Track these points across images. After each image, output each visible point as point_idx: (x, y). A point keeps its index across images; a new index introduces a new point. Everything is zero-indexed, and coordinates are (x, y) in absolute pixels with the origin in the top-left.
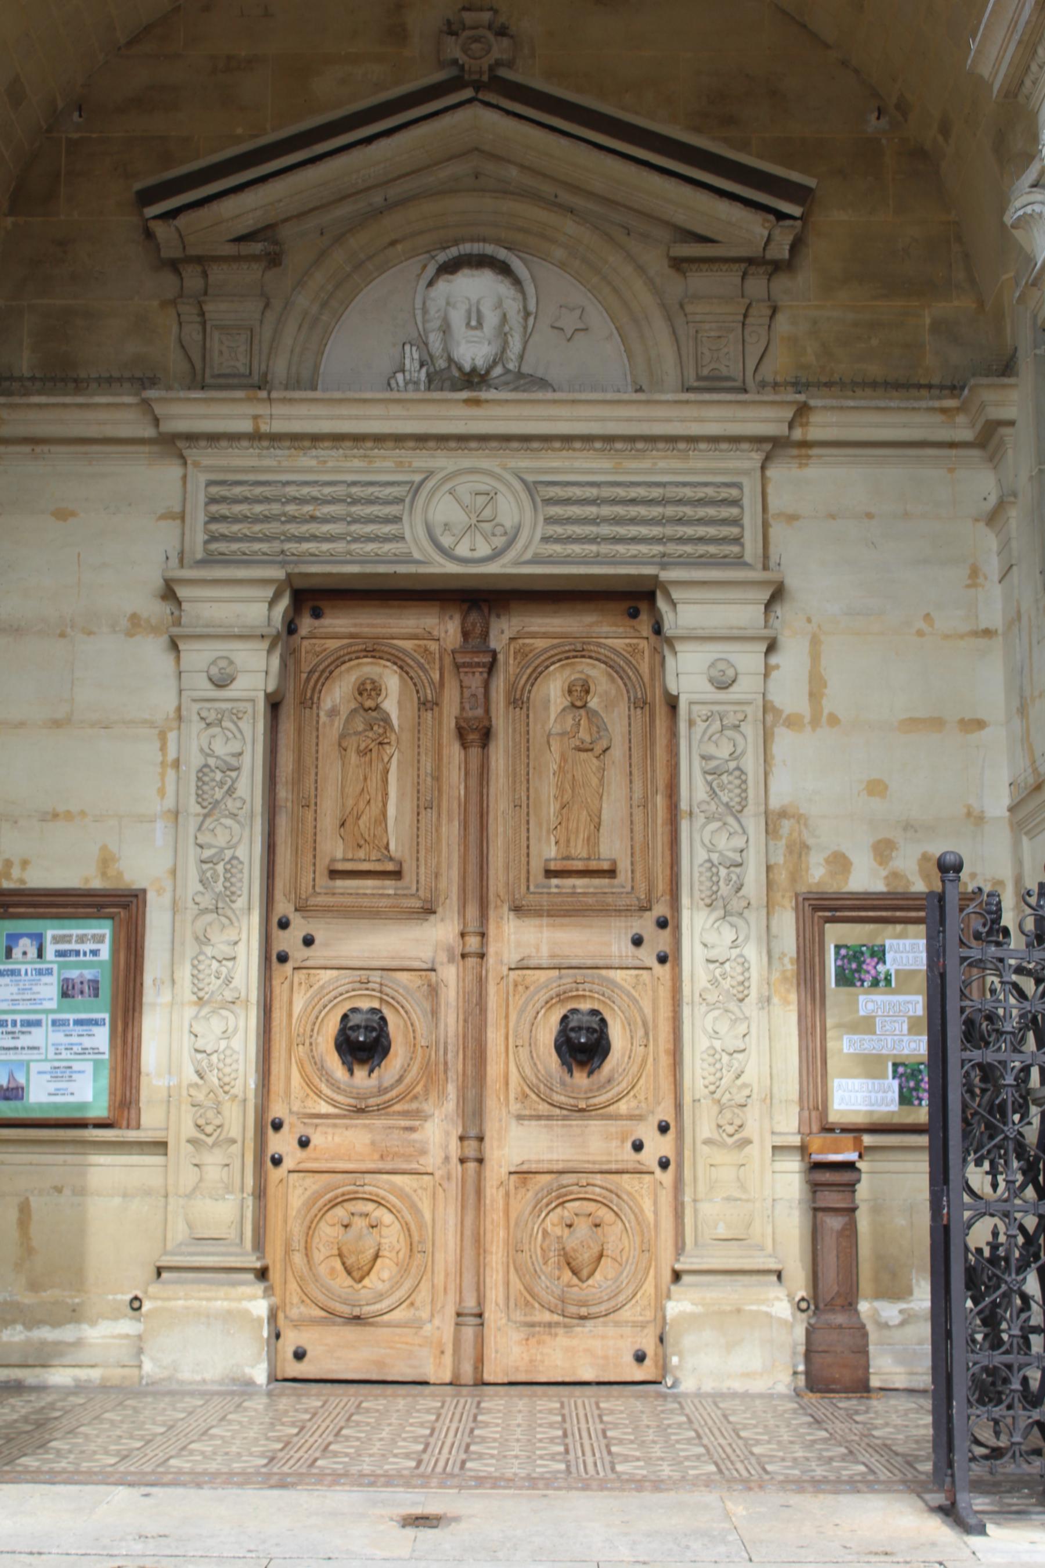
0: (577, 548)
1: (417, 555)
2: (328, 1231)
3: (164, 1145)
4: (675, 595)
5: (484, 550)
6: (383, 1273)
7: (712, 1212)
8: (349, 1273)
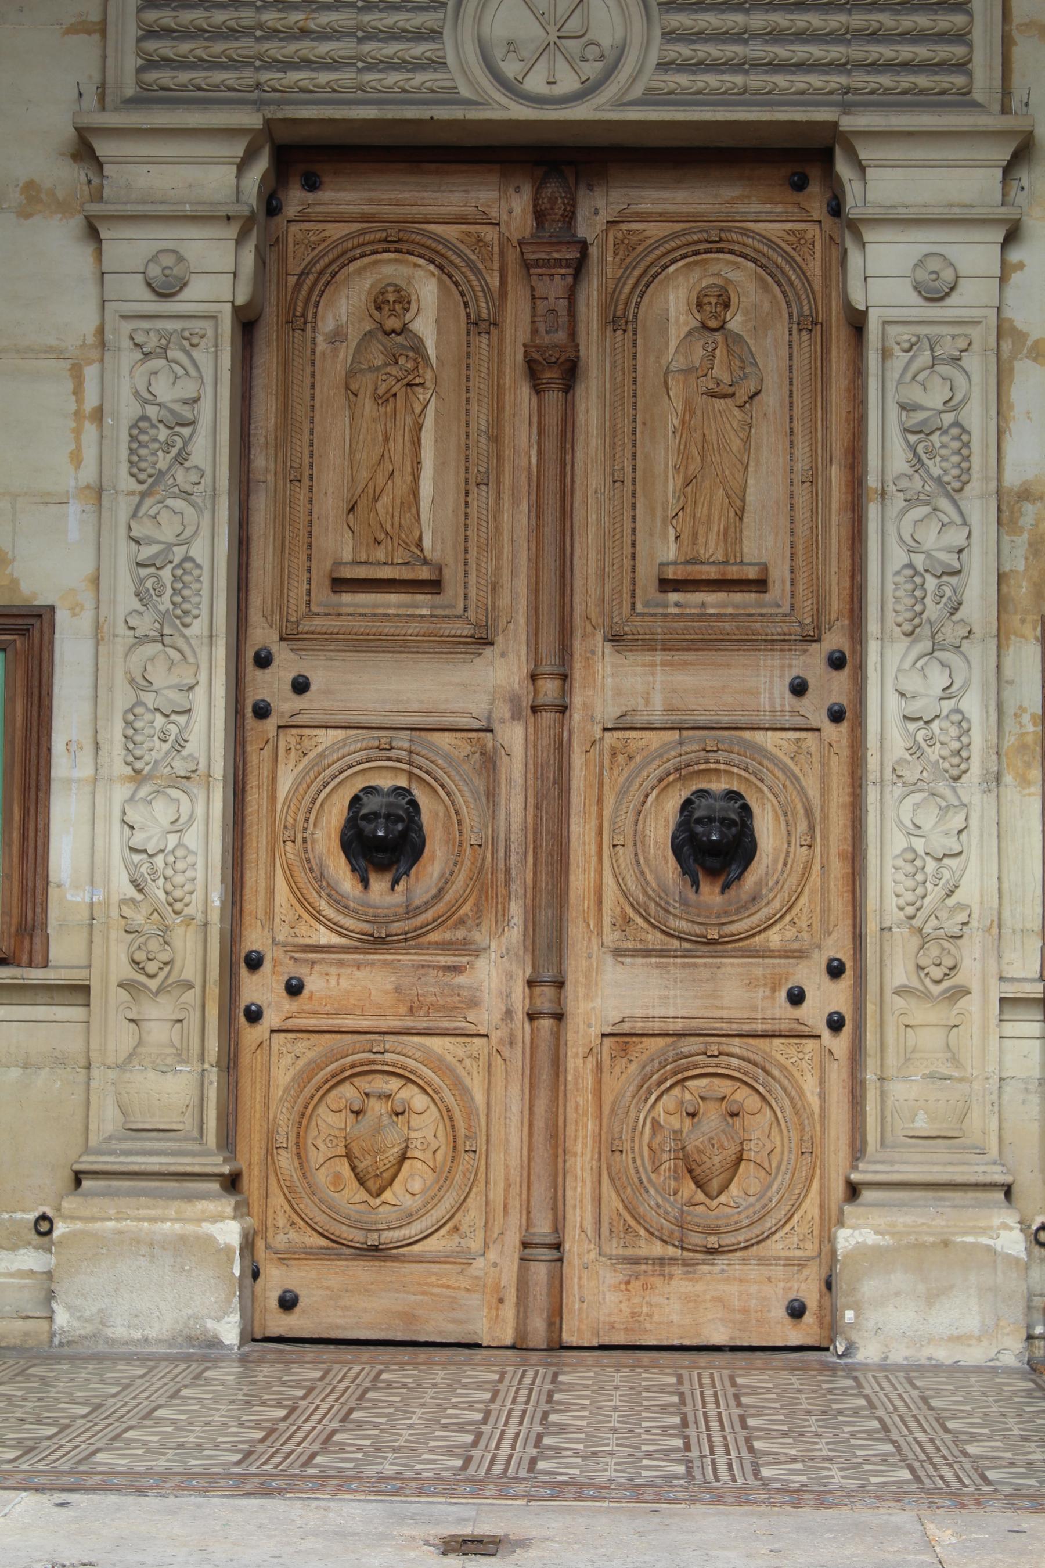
0: (712, 80)
1: (465, 92)
2: (330, 1120)
3: (85, 989)
4: (864, 154)
5: (568, 83)
6: (415, 1179)
7: (907, 1099)
8: (362, 1182)
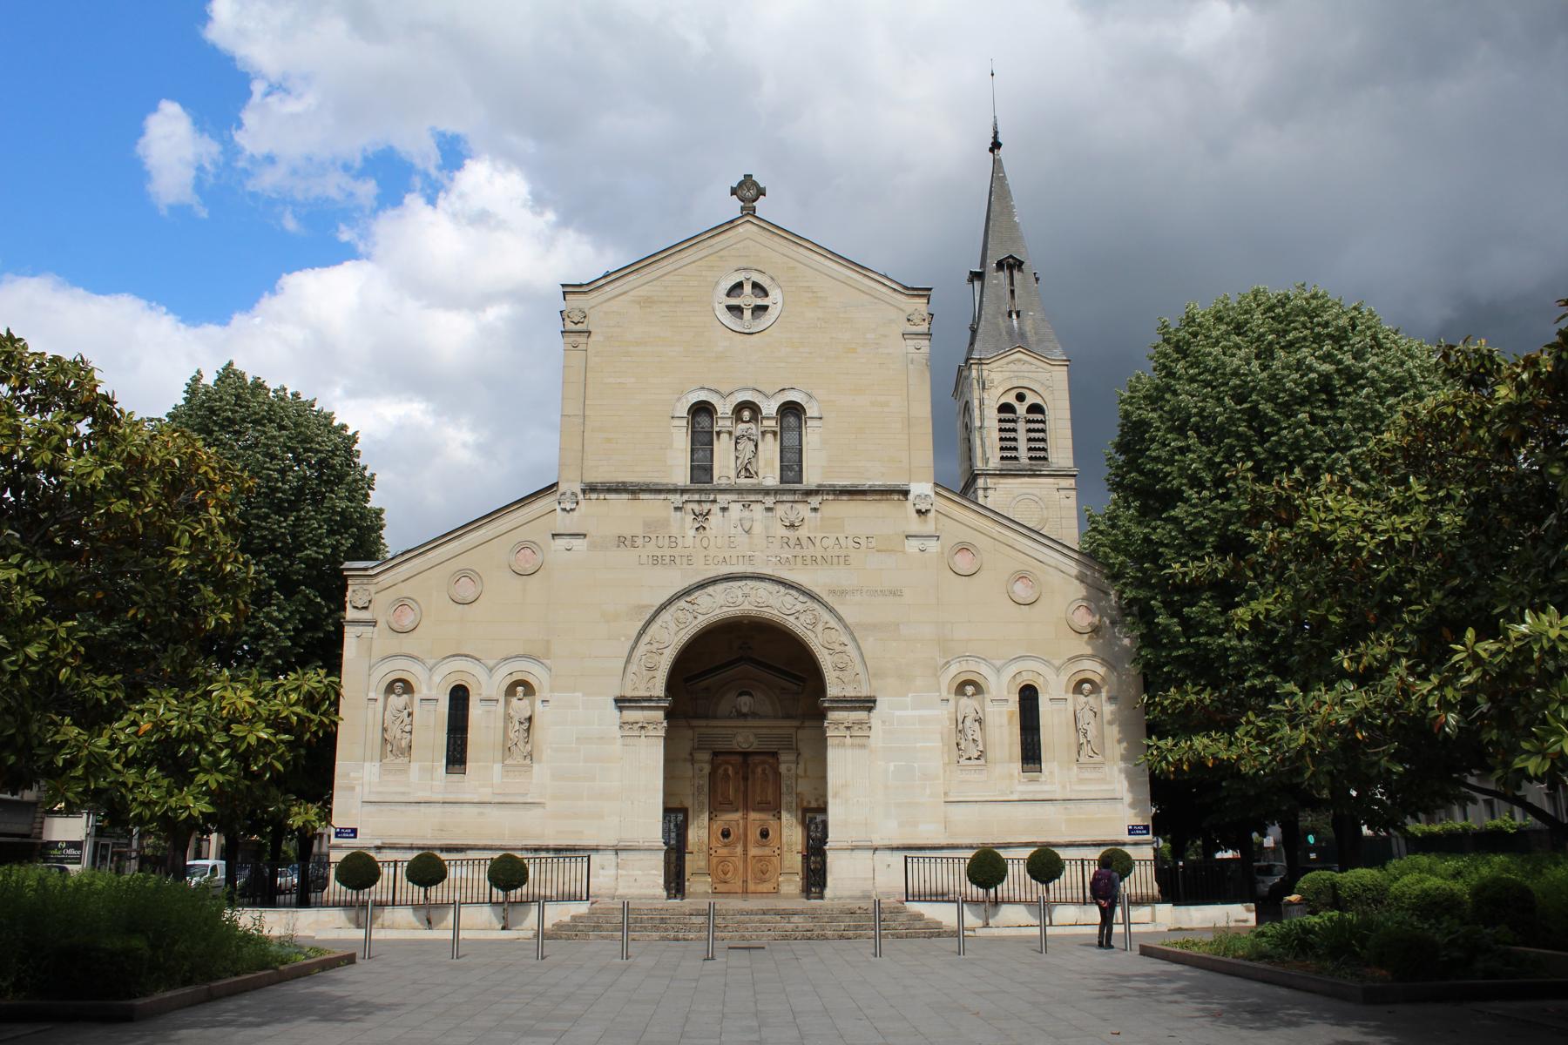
7: (786, 863)
